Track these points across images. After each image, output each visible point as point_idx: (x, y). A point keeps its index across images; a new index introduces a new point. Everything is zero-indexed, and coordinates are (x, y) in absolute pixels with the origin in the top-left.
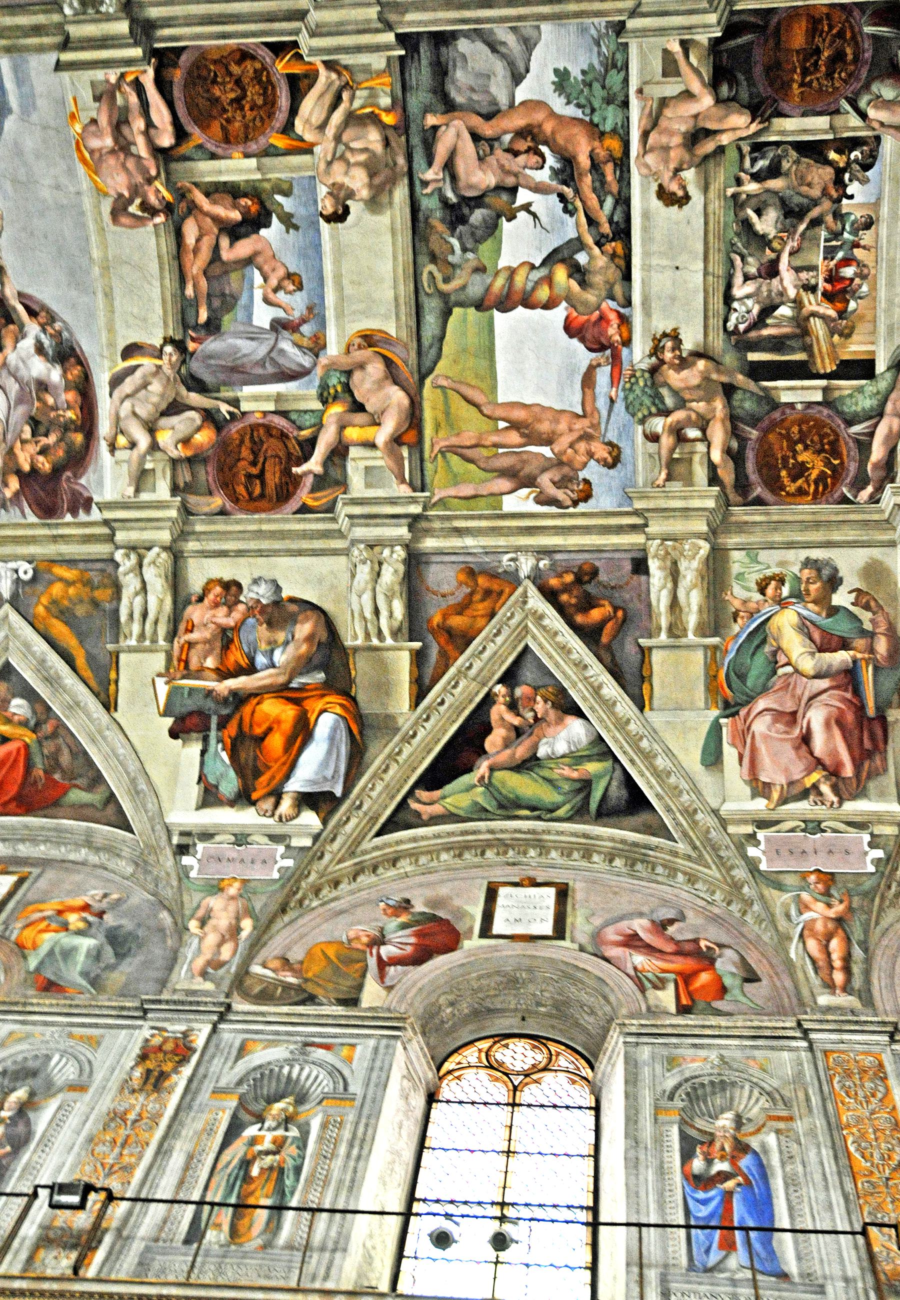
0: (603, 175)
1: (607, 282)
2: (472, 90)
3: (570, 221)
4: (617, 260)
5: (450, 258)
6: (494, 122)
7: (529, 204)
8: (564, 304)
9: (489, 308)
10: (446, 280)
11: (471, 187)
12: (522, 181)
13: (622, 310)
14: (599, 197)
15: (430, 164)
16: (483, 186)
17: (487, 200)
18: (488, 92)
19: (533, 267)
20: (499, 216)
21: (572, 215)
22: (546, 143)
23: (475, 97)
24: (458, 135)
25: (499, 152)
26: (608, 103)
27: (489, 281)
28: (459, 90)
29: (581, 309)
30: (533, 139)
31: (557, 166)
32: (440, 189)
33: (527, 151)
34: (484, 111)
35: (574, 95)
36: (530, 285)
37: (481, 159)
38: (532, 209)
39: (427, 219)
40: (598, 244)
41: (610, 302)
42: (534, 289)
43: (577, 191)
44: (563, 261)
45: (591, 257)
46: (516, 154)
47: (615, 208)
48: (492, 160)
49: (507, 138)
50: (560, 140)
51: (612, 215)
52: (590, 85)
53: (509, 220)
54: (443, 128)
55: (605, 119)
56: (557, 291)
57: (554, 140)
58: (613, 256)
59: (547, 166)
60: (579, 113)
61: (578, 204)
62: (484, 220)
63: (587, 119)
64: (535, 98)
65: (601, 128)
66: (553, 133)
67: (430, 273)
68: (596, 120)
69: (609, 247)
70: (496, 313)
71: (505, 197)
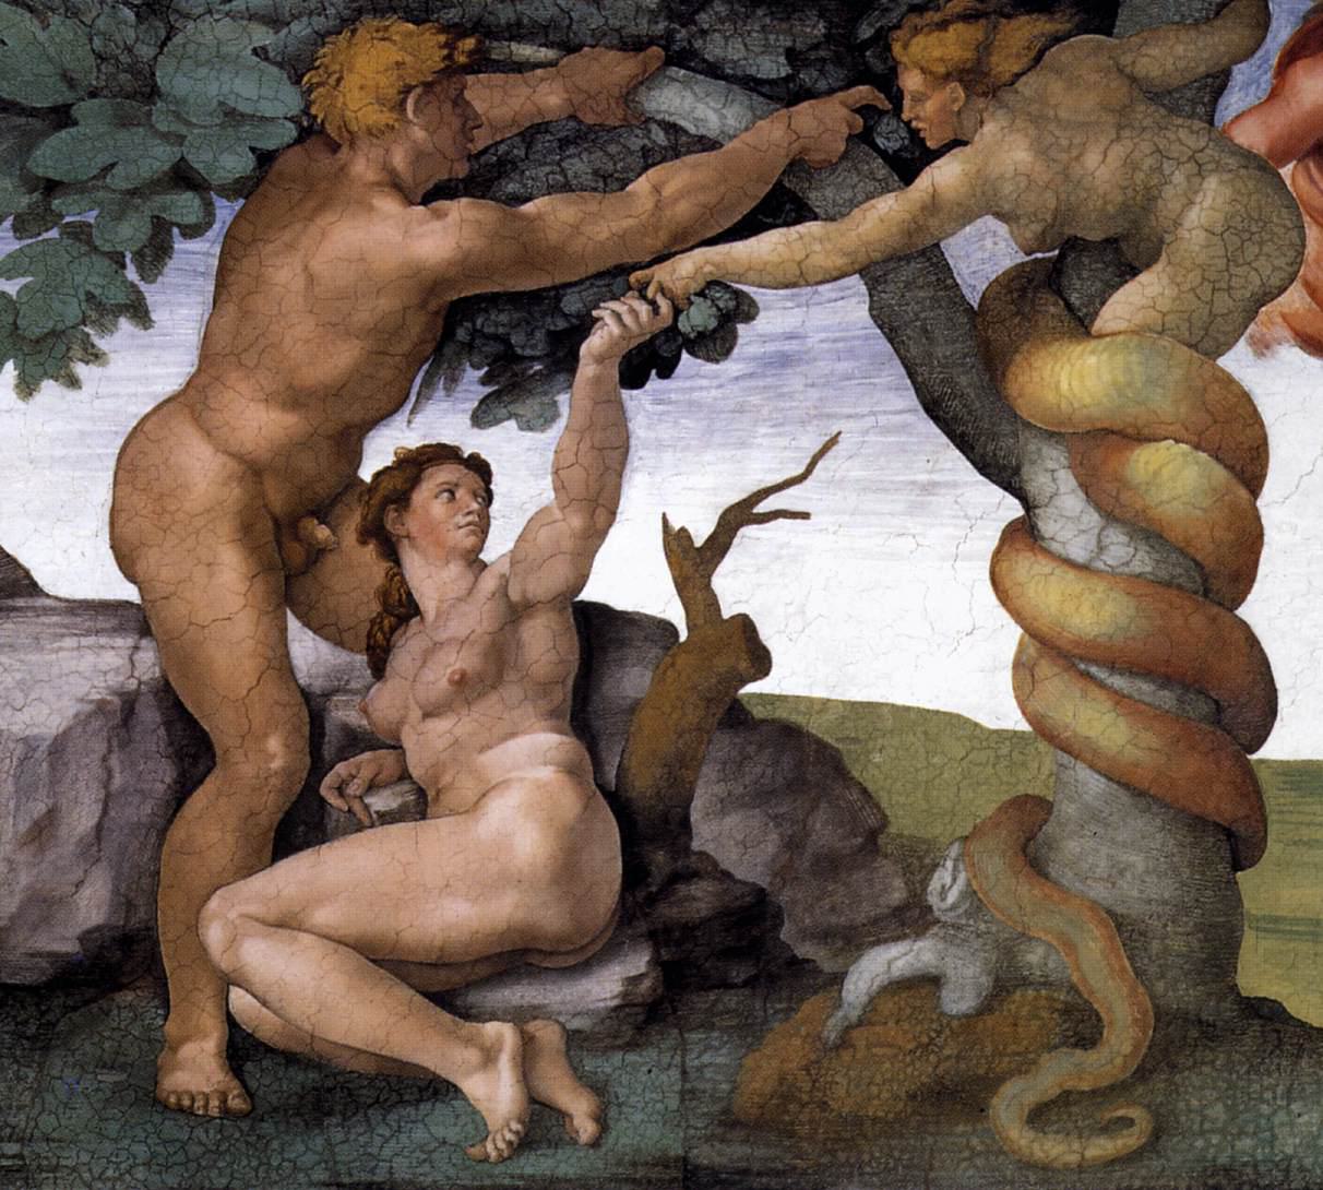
0: (532, 133)
1: (1122, 120)
2: (42, 831)
3: (775, 317)
4: (1004, 64)
5: (959, 1000)
6: (221, 726)
7: (676, 542)
8: (1238, 362)
9: (1248, 783)
10: (1083, 1027)
11: (567, 868)
12: (546, 582)
13: (1281, 32)
14: (649, 158)
15: (438, 1089)
16: (569, 802)
17: (644, 783)
18: (59, 747)
19: (1023, 534)
20: (736, 716)
21: (741, 310)
22: (349, 443)
23: (82, 818)
24: (286, 923)
25: (386, 702)
26: (151, 93)
27: (1093, 784)
28: (43, 906)
29: (1267, 269)
30: (322, 513)
31: (472, 384)
32: (575, 1040)
33: (390, 550)
34: (162, 775)
35: (91, 275)
36: (1120, 549)
37: (421, 805)
38: (701, 531)
39: (729, 1122)
40: (908, 163)
41: (1234, 101)
42: (1147, 532)
43: (616, 277)
44: (994, 363)
45: (983, 201)
46: (401, 609)
47: (714, 71)
48: (426, 743)
49: (308, 651)
50: (341, 358)
51: (751, 84)
52: (51, 187)
53: (761, 662)
54: (239, 999)
55: (232, 116)
56: (1164, 404)
57: (335, 392)
58: (977, 80)
59: (473, 442)
60: (197, 255)
61: (687, 268)
62: (761, 797)
63: (225, 211)
64: (102, 493)
65: (291, 131)
66: (294, 398)
67: (1039, 1117)
68: (235, 163)
69: (926, 103)
70: (1280, 746)
71: (631, 680)
